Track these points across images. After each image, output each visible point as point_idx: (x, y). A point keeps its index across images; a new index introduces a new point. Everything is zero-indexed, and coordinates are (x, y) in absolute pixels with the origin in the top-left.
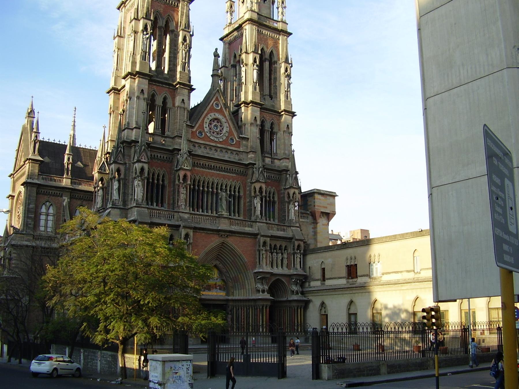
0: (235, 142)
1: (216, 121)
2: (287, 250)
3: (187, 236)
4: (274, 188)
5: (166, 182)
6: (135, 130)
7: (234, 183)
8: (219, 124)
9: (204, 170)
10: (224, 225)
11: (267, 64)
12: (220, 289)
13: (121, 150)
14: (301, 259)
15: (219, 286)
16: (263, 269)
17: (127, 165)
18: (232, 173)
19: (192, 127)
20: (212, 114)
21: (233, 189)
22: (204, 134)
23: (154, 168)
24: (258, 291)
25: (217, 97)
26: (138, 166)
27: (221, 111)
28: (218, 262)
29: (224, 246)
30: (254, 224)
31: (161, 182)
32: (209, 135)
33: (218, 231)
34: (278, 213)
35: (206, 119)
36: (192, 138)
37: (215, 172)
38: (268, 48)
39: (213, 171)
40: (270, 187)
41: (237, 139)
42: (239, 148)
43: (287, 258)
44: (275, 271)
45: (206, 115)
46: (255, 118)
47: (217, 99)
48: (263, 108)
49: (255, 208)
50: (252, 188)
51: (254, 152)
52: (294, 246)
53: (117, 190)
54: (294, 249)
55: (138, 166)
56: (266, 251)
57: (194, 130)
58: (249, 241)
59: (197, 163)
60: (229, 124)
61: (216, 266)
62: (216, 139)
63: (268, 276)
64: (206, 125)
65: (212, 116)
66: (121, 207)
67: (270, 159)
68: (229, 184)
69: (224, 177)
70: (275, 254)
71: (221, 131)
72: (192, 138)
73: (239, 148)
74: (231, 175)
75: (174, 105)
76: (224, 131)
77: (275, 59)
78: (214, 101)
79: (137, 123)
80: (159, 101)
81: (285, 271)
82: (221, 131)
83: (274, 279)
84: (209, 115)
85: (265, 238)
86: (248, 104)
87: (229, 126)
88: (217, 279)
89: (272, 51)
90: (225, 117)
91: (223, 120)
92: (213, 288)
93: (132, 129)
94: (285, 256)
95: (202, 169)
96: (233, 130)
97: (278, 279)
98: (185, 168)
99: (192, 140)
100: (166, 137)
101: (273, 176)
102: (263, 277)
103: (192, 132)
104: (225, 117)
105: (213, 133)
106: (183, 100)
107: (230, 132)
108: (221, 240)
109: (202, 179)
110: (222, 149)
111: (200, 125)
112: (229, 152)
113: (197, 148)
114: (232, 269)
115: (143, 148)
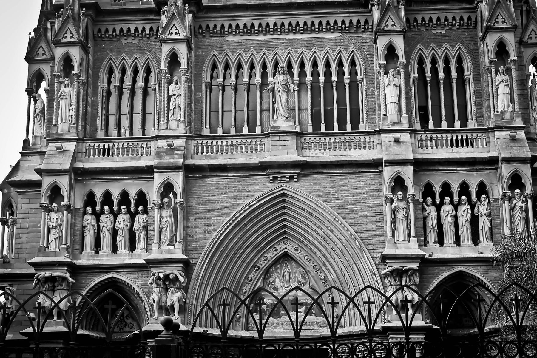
2: (487, 193)
3: (168, 188)
4: (459, 45)
10: (284, 152)
14: (527, 211)
18: (328, 31)
29: (292, 204)
37: (282, 37)
39: (276, 37)
40: (446, 45)
43: (489, 215)
44: (449, 251)
59: (230, 26)
63: (415, 265)
69: (307, 44)
70: (447, 208)
74: (329, 35)
81: (487, 249)
83: (444, 274)
97: (461, 272)
98: (174, 36)
114: (328, 260)
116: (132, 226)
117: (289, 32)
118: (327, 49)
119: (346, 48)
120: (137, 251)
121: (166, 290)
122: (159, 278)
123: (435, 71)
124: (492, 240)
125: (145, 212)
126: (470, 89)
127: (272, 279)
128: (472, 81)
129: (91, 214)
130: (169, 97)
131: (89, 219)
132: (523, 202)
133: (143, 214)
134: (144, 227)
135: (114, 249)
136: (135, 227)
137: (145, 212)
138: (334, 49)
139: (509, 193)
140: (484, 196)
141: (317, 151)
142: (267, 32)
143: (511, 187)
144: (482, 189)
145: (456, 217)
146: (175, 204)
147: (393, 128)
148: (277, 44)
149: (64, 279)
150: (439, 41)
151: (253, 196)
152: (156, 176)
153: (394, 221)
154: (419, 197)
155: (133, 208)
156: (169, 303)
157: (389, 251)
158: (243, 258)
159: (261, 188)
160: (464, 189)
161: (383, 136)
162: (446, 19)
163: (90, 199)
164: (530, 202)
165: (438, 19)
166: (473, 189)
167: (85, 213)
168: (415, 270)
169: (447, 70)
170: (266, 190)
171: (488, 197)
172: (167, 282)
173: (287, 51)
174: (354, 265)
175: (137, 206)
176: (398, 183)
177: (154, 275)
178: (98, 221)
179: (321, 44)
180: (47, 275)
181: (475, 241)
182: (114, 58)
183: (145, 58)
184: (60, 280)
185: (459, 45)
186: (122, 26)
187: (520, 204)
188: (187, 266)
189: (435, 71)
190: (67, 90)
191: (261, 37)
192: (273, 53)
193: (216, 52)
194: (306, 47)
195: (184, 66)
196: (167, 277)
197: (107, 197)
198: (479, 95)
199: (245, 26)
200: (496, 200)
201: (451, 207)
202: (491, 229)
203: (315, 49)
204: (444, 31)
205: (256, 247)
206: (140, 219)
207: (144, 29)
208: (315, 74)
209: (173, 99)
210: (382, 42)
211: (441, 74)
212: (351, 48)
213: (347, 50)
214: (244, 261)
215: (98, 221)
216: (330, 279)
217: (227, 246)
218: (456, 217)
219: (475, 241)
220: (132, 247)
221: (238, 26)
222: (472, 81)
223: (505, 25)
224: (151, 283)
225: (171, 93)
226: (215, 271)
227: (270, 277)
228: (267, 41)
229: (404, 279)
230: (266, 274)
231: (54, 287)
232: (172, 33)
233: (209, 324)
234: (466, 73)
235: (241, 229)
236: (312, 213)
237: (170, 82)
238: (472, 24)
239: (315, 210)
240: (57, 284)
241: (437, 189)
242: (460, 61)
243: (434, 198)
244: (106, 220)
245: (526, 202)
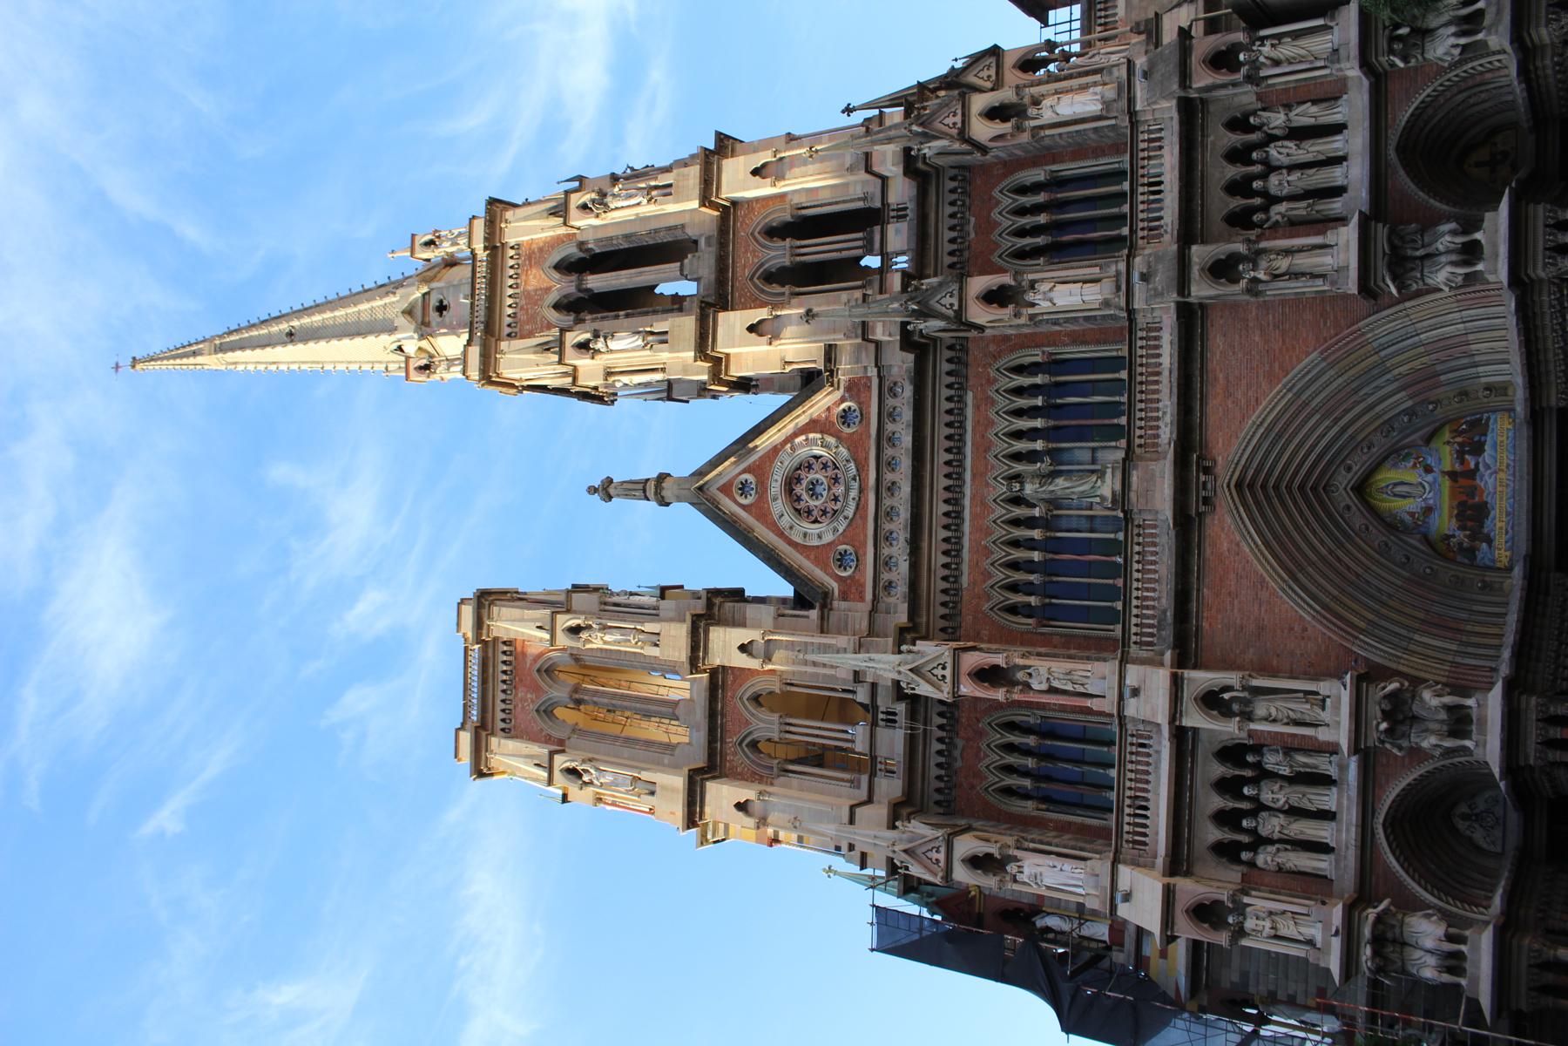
2: (1246, 116)
3: (1212, 701)
4: (996, 193)
7: (1003, 403)
11: (598, 282)
12: (1478, 449)
14: (1279, 37)
15: (1460, 455)
16: (1341, 270)
21: (1023, 402)
22: (842, 547)
23: (982, 766)
24: (1470, 279)
27: (761, 470)
28: (1343, 481)
29: (1258, 471)
30: (1141, 321)
33: (1187, 524)
37: (968, 491)
38: (548, 289)
39: (967, 502)
40: (995, 215)
41: (838, 395)
44: (1355, 174)
47: (726, 489)
48: (718, 299)
52: (1224, 86)
54: (1235, 85)
56: (1254, 258)
58: (1218, 343)
59: (945, 578)
61: (1361, 488)
62: (853, 493)
63: (1381, 232)
67: (891, 229)
68: (1004, 424)
72: (862, 599)
74: (969, 412)
77: (572, 250)
80: (766, 724)
81: (1354, 108)
82: (825, 466)
83: (1402, 179)
84: (785, 522)
85: (1195, 271)
86: (717, 362)
88: (1428, 470)
89: (558, 267)
92: (1473, 491)
94: (1277, 120)
97: (1400, 149)
99: (869, 596)
101: (949, 210)
102: (1392, 259)
103: (844, 596)
105: (836, 499)
108: (1225, 501)
111: (818, 562)
112: (890, 427)
116: (1283, 777)
117: (960, 477)
118: (992, 414)
119: (991, 382)
120: (1333, 772)
121: (1415, 719)
122: (1386, 731)
123: (1036, 230)
124: (1337, 98)
125: (1257, 749)
126: (1069, 168)
127: (1407, 518)
128: (1055, 168)
129: (1256, 853)
130: (1052, 690)
131: (1264, 858)
132: (1263, 45)
133: (1262, 755)
134: (1286, 754)
135: (1327, 815)
136: (1286, 771)
137: (1257, 749)
138: (993, 402)
139: (1244, 70)
140: (1252, 120)
141: (1160, 423)
143: (1234, 66)
144: (1239, 124)
145: (1292, 168)
146: (1244, 688)
147: (1124, 287)
148: (979, 500)
149: (1379, 919)
150: (987, 226)
151: (1238, 545)
152: (1187, 722)
153: (1294, 275)
154: (1253, 234)
155: (1248, 773)
156: (1443, 715)
157: (1352, 287)
158: (1360, 571)
159: (1229, 532)
160: (1237, 156)
161: (1138, 304)
162: (952, 216)
163: (1226, 852)
164: (1263, 33)
165: (952, 228)
166: (1237, 139)
167: (1252, 864)
168: (1392, 232)
169: (1036, 209)
170: (1229, 520)
171: (1254, 113)
172: (1400, 713)
173: (991, 482)
174: (1383, 354)
175: (1246, 765)
176: (1223, 270)
177: (1383, 742)
178: (1269, 841)
179: (984, 424)
180: (1368, 951)
181: (1338, 128)
182: (984, 784)
183: (988, 728)
184: (1381, 927)
186: (932, 764)
187: (1266, 49)
188: (1368, 676)
189: (1036, 230)
190: (1026, 870)
191: (967, 527)
192: (993, 505)
193: (986, 606)
194: (987, 450)
195: (999, 660)
196: (1386, 715)
197: (1224, 818)
198: (1079, 152)
199: (946, 553)
200: (1259, 97)
201: (1274, 180)
202: (1314, 102)
203: (990, 435)
204: (973, 219)
205: (1340, 545)
206: (1272, 761)
207: (941, 727)
208: (1032, 434)
209: (1056, 684)
210: (979, 314)
211: (1042, 219)
212: (992, 374)
213: (996, 380)
214: (1367, 569)
215: (1269, 841)
216: (1410, 403)
217: (1335, 598)
218: (1292, 168)
219: (1338, 128)
220: (1325, 781)
221: (945, 566)
222: (1055, 168)
223: (959, 112)
224: (1400, 748)
225: (1044, 687)
226: (1383, 623)
227: (1402, 521)
228: (974, 517)
229: (1409, 252)
230: (1397, 529)
231: (1394, 941)
232: (944, 677)
233: (1495, 642)
234: (1042, 178)
235: (1301, 569)
236: (1277, 433)
237: (1027, 686)
238: (964, 173)
239: (1269, 430)
240: (1389, 935)
241: (1237, 203)
242: (1022, 190)
243: (1254, 210)
244: (1271, 825)
245: (1263, 39)
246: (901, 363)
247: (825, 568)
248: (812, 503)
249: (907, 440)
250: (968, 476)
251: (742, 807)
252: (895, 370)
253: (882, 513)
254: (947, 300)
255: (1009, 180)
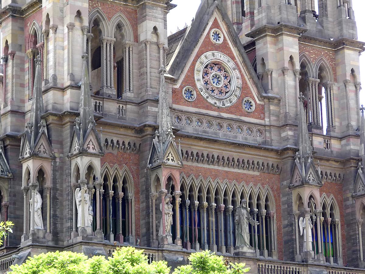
0: (253, 108)
1: (216, 68)
5: (131, 195)
6: (69, 92)
7: (256, 190)
8: (223, 72)
9: (200, 165)
13: (43, 133)
17: (58, 160)
19: (174, 81)
20: (209, 53)
22: (194, 93)
25: (216, 20)
26: (82, 162)
27: (224, 48)
31: (121, 194)
32: (204, 95)
34: (343, 246)
35: (198, 64)
36: (174, 102)
37: (220, 168)
39: (216, 167)
41: (258, 102)
42: (263, 119)
45: (198, 56)
46: (291, 58)
47: (216, 25)
48: (305, 38)
49: (302, 237)
50: (294, 198)
51: (295, 126)
53: (40, 212)
55: (82, 162)
57: (177, 86)
60: (240, 72)
64: (198, 76)
65: (209, 57)
66: (51, 244)
71: (226, 86)
72: (174, 102)
73: (263, 119)
74: (251, 173)
75: (136, 38)
76: (233, 87)
78: (211, 29)
79: (72, 76)
82: (226, 86)
84: (203, 57)
87: (242, 75)
90: (233, 58)
91: (230, 65)
93: (63, 90)
95: (195, 164)
96: (250, 83)
98: (170, 162)
100: (126, 103)
103: (174, 91)
104: (233, 58)
105: (213, 91)
106: (155, 29)
107: (244, 88)
109: (197, 183)
110: (233, 123)
111: (187, 76)
113: (184, 122)
115: (90, 126)
118: (251, 184)
119: (263, 184)
142: (213, 163)
179: (247, 179)
183: (123, 169)
185: (332, 196)
191: (206, 166)
212: (266, 186)
213: (264, 187)
246: (275, 140)
247: (185, 82)
248: (210, 76)
249: (240, 139)
250: (226, 169)
251: (79, 13)
252: (268, 135)
253: (210, 118)
254: (311, 178)
255: (336, 203)
